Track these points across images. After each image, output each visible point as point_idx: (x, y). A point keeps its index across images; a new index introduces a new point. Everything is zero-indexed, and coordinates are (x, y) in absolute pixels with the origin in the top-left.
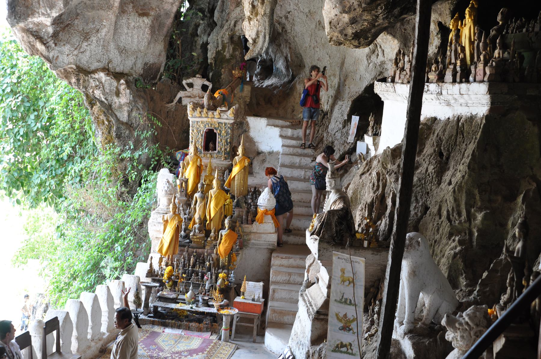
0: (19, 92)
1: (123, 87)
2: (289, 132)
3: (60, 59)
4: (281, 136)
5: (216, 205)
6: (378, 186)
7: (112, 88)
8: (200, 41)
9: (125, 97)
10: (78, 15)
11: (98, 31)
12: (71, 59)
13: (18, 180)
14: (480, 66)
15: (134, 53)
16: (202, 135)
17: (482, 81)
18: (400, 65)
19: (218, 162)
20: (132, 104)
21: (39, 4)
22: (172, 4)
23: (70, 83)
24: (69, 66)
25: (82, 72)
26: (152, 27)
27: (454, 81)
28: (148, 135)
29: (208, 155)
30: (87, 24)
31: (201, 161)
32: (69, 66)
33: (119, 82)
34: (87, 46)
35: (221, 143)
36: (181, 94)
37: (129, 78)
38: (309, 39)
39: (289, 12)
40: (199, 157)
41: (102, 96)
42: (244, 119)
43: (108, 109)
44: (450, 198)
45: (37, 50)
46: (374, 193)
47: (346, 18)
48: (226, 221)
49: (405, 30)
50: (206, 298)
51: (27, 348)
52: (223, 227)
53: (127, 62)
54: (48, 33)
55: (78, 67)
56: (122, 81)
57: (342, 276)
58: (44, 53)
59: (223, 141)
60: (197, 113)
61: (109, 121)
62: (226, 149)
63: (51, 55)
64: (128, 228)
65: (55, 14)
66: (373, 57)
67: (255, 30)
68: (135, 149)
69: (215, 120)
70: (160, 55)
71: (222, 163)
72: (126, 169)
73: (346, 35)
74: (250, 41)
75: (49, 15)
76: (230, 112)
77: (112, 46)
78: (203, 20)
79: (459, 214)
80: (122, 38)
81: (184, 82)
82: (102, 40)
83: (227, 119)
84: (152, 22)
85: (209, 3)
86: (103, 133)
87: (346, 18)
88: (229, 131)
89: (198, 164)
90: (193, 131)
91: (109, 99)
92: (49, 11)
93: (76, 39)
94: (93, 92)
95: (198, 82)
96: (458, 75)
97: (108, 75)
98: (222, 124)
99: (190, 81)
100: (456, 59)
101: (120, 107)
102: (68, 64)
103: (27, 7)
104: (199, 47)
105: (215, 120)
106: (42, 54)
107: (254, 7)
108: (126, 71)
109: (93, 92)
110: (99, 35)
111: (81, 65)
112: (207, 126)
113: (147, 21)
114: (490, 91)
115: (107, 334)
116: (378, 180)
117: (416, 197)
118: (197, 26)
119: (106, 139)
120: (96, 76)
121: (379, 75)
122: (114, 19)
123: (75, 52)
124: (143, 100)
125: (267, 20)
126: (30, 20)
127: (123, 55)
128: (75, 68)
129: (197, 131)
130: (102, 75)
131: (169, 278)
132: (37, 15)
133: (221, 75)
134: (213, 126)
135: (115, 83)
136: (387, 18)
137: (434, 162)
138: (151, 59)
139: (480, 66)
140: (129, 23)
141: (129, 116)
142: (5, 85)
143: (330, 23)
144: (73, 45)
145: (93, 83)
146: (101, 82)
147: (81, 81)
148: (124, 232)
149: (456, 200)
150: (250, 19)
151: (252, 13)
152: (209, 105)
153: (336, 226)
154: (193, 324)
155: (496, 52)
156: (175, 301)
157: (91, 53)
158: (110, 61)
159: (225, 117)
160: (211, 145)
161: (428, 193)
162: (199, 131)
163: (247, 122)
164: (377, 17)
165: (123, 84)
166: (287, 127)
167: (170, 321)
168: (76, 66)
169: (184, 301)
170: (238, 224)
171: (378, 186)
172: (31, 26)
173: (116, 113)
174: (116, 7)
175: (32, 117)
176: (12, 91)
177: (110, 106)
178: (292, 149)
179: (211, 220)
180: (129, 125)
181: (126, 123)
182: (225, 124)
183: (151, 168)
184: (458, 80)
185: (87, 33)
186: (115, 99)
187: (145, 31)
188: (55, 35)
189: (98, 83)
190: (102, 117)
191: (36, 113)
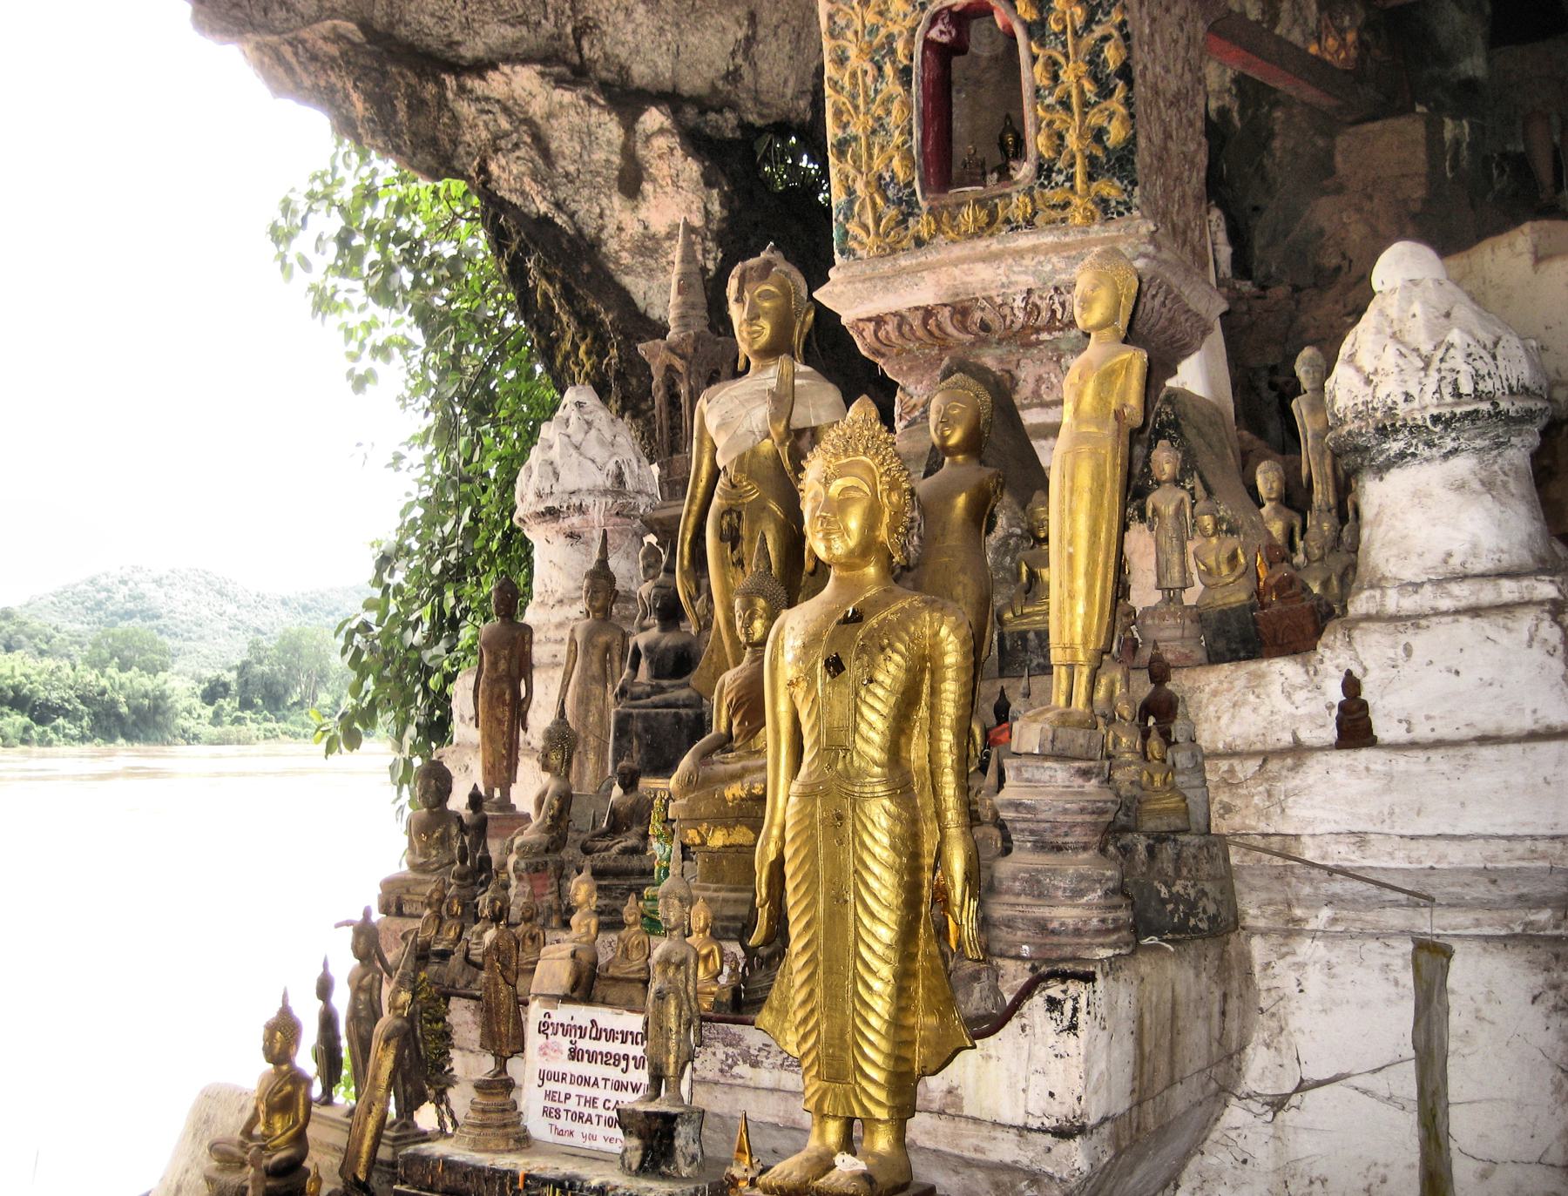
7: (599, 156)
16: (905, 74)
29: (968, 216)
33: (635, 119)
37: (712, 116)
41: (530, 186)
59: (1068, 76)
101: (648, 246)
111: (402, 31)
120: (495, 84)
133: (1271, 135)
135: (610, 129)
165: (662, 131)
173: (627, 281)
189: (505, 124)
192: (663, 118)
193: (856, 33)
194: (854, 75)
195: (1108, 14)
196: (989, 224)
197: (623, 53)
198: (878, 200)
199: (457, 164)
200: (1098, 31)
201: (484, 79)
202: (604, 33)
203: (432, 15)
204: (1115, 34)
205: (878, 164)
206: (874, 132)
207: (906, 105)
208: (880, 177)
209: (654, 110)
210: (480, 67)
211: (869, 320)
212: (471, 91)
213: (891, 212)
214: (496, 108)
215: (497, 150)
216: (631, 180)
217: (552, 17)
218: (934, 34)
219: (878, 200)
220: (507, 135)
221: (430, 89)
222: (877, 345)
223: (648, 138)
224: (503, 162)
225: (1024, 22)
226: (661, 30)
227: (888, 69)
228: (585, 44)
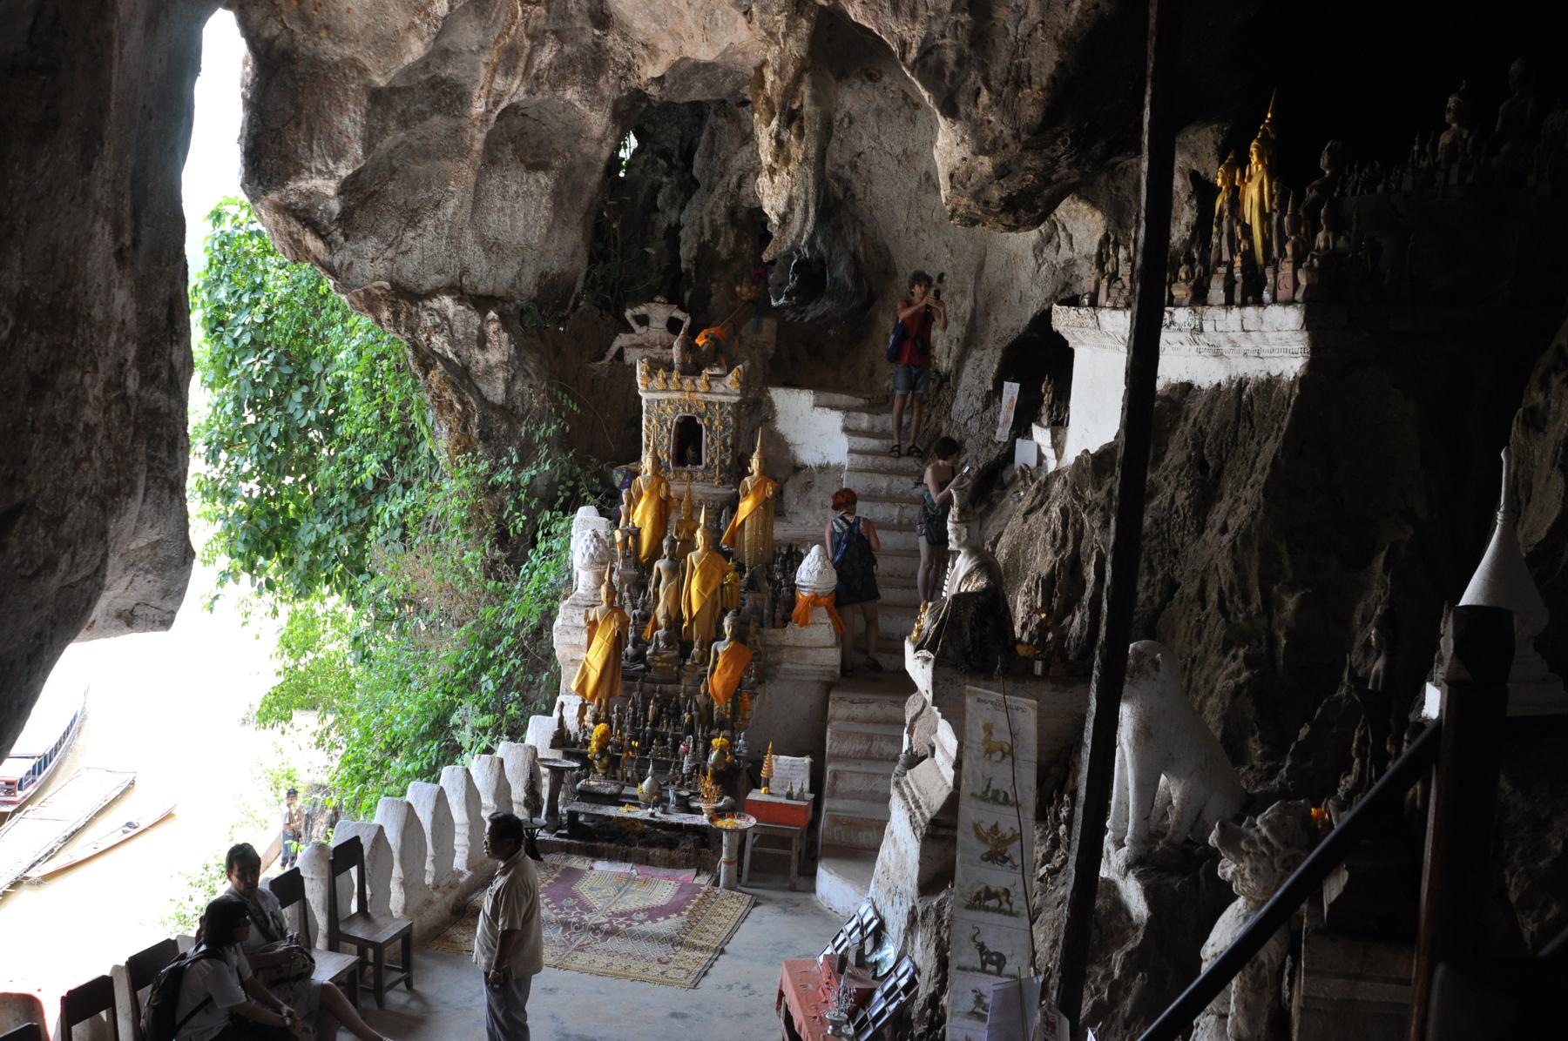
0: (269, 344)
1: (493, 327)
2: (864, 421)
3: (357, 269)
4: (846, 430)
5: (704, 586)
6: (1065, 539)
8: (663, 223)
9: (498, 352)
10: (394, 171)
11: (437, 205)
12: (380, 268)
13: (268, 536)
14: (1286, 268)
15: (518, 250)
16: (669, 431)
17: (1290, 302)
18: (1109, 267)
19: (707, 490)
20: (514, 366)
21: (311, 150)
22: (600, 142)
23: (378, 321)
24: (376, 283)
25: (402, 298)
26: (556, 196)
27: (1229, 303)
28: (550, 432)
29: (685, 475)
30: (415, 190)
31: (668, 487)
32: (376, 283)
35: (712, 447)
36: (622, 340)
38: (905, 213)
39: (859, 155)
40: (663, 480)
42: (764, 393)
43: (462, 376)
44: (1224, 563)
45: (308, 251)
46: (1056, 553)
47: (986, 164)
48: (727, 622)
49: (1118, 189)
50: (684, 793)
51: (296, 904)
52: (720, 636)
54: (331, 214)
55: (394, 285)
56: (492, 314)
57: (987, 741)
58: (321, 257)
59: (717, 443)
60: (657, 382)
61: (464, 404)
62: (722, 462)
63: (336, 261)
64: (508, 640)
65: (344, 171)
66: (1049, 252)
67: (785, 193)
68: (523, 464)
69: (698, 396)
70: (574, 254)
71: (715, 491)
72: (502, 507)
73: (987, 203)
74: (775, 219)
75: (331, 175)
76: (730, 377)
77: (469, 236)
78: (668, 175)
79: (1246, 598)
80: (490, 219)
81: (628, 314)
82: (446, 226)
83: (725, 394)
84: (557, 181)
85: (682, 139)
86: (451, 429)
87: (986, 164)
89: (663, 494)
90: (649, 421)
91: (464, 353)
92: (332, 166)
93: (389, 226)
94: (428, 339)
95: (659, 312)
96: (1238, 287)
97: (460, 301)
98: (714, 404)
99: (642, 310)
100: (1232, 252)
101: (489, 370)
103: (286, 158)
104: (660, 235)
105: (698, 396)
106: (317, 259)
107: (780, 144)
108: (500, 292)
109: (428, 339)
110: (440, 214)
113: (544, 179)
114: (1309, 323)
115: (468, 874)
116: (1065, 525)
117: (1150, 562)
118: (656, 188)
119: (458, 442)
120: (435, 304)
121: (1063, 290)
122: (472, 178)
123: (389, 254)
124: (538, 356)
125: (810, 173)
126: (291, 185)
127: (494, 257)
129: (659, 421)
130: (447, 301)
131: (602, 750)
132: (307, 174)
133: (710, 295)
135: (477, 320)
136: (1076, 163)
137: (1188, 482)
138: (555, 264)
139: (1286, 268)
140: (505, 187)
141: (508, 390)
142: (240, 330)
143: (951, 176)
144: (383, 238)
145: (428, 321)
146: (446, 318)
147: (403, 317)
148: (500, 649)
149: (1237, 566)
150: (772, 172)
151: (776, 157)
152: (684, 363)
153: (972, 629)
154: (657, 851)
155: (1321, 236)
156: (615, 800)
157: (422, 252)
158: (465, 271)
159: (721, 389)
160: (690, 452)
161: (1176, 552)
162: (662, 422)
163: (770, 399)
164: (1056, 161)
166: (858, 409)
167: (605, 845)
169: (635, 801)
170: (752, 628)
171: (1065, 539)
172: (293, 199)
175: (297, 397)
176: (253, 341)
177: (466, 369)
178: (870, 458)
179: (692, 620)
180: (508, 411)
181: (502, 407)
182: (721, 405)
183: (557, 506)
184: (1238, 299)
185: (415, 211)
186: (478, 355)
187: (540, 202)
188: (345, 218)
190: (449, 395)
191: (305, 389)
216: (482, 342)
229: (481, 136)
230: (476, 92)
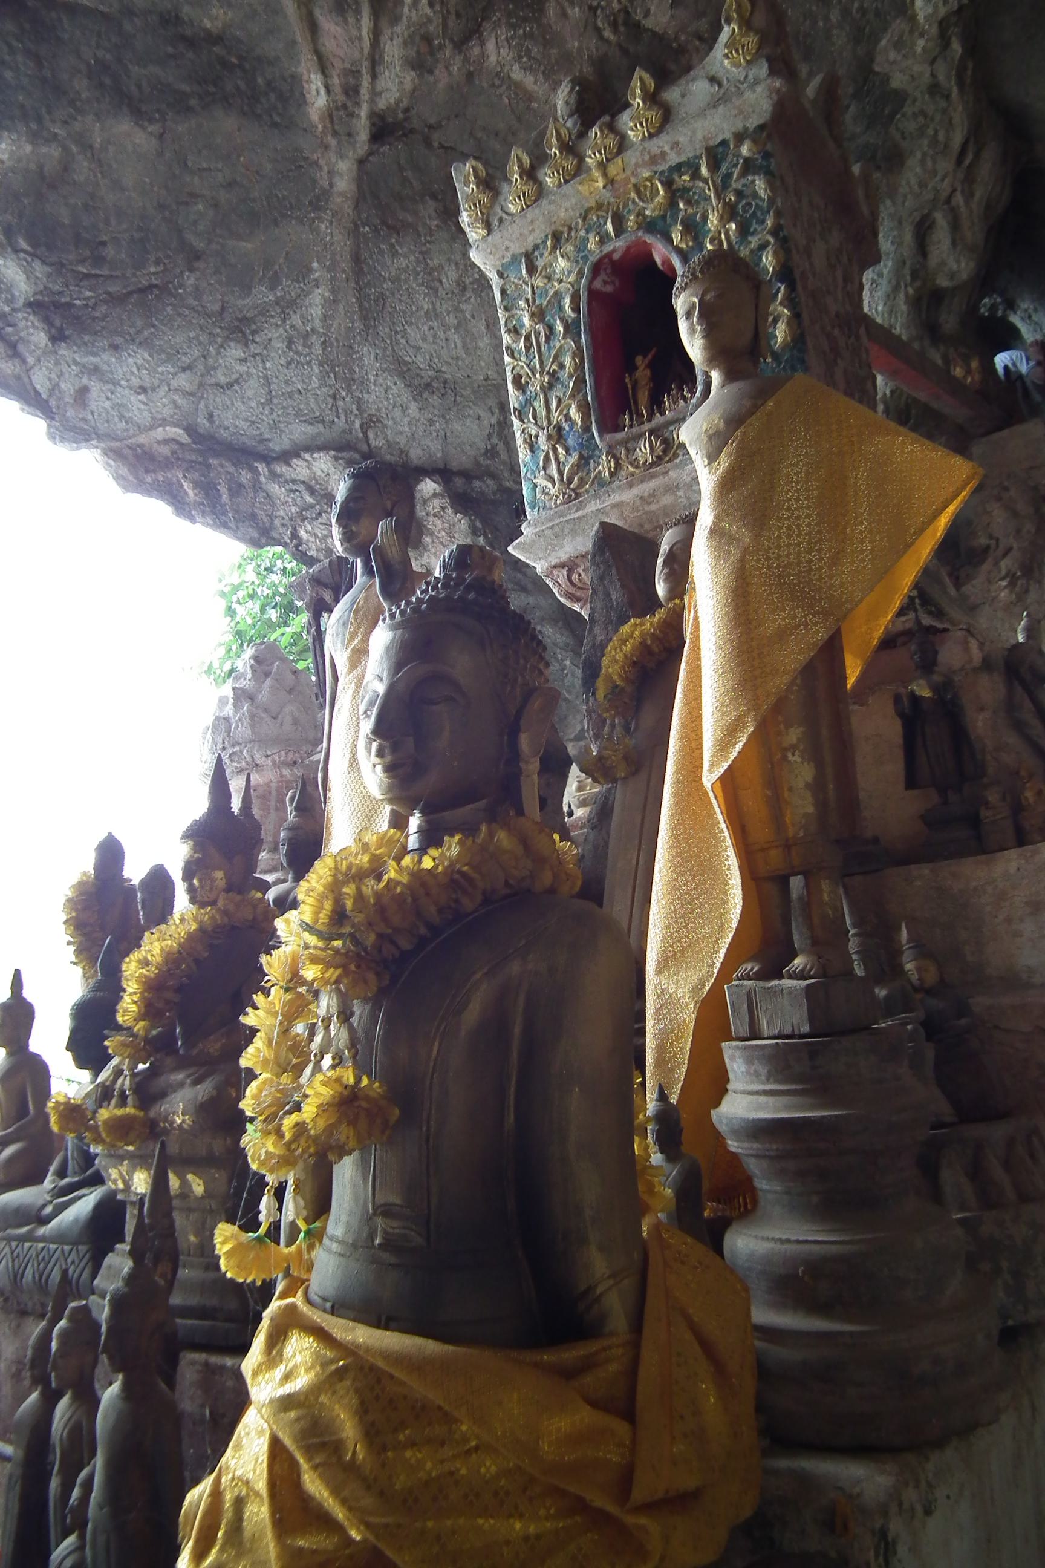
16: (571, 329)
24: (159, 433)
32: (159, 433)
34: (244, 360)
37: (477, 484)
53: (457, 426)
88: (760, 185)
102: (152, 428)
110: (296, 319)
112: (592, 244)
120: (299, 469)
123: (183, 381)
127: (435, 400)
128: (185, 439)
129: (539, 315)
134: (631, 221)
147: (223, 489)
165: (435, 495)
168: (190, 430)
174: (342, 194)
182: (716, 155)
189: (309, 500)
192: (436, 486)
193: (527, 301)
194: (528, 338)
195: (763, 222)
196: (665, 451)
197: (402, 440)
198: (560, 450)
199: (274, 534)
200: (754, 241)
201: (290, 465)
202: (386, 426)
203: (246, 420)
204: (772, 241)
205: (555, 417)
206: (551, 386)
207: (578, 353)
208: (559, 428)
209: (428, 480)
210: (286, 457)
211: (562, 565)
212: (280, 476)
213: (574, 458)
214: (302, 488)
215: (303, 519)
217: (343, 417)
218: (598, 284)
219: (560, 450)
220: (312, 506)
221: (245, 477)
222: (571, 590)
223: (425, 502)
224: (309, 528)
225: (679, 251)
226: (431, 422)
227: (560, 328)
228: (371, 434)
229: (345, 167)
230: (302, 69)
